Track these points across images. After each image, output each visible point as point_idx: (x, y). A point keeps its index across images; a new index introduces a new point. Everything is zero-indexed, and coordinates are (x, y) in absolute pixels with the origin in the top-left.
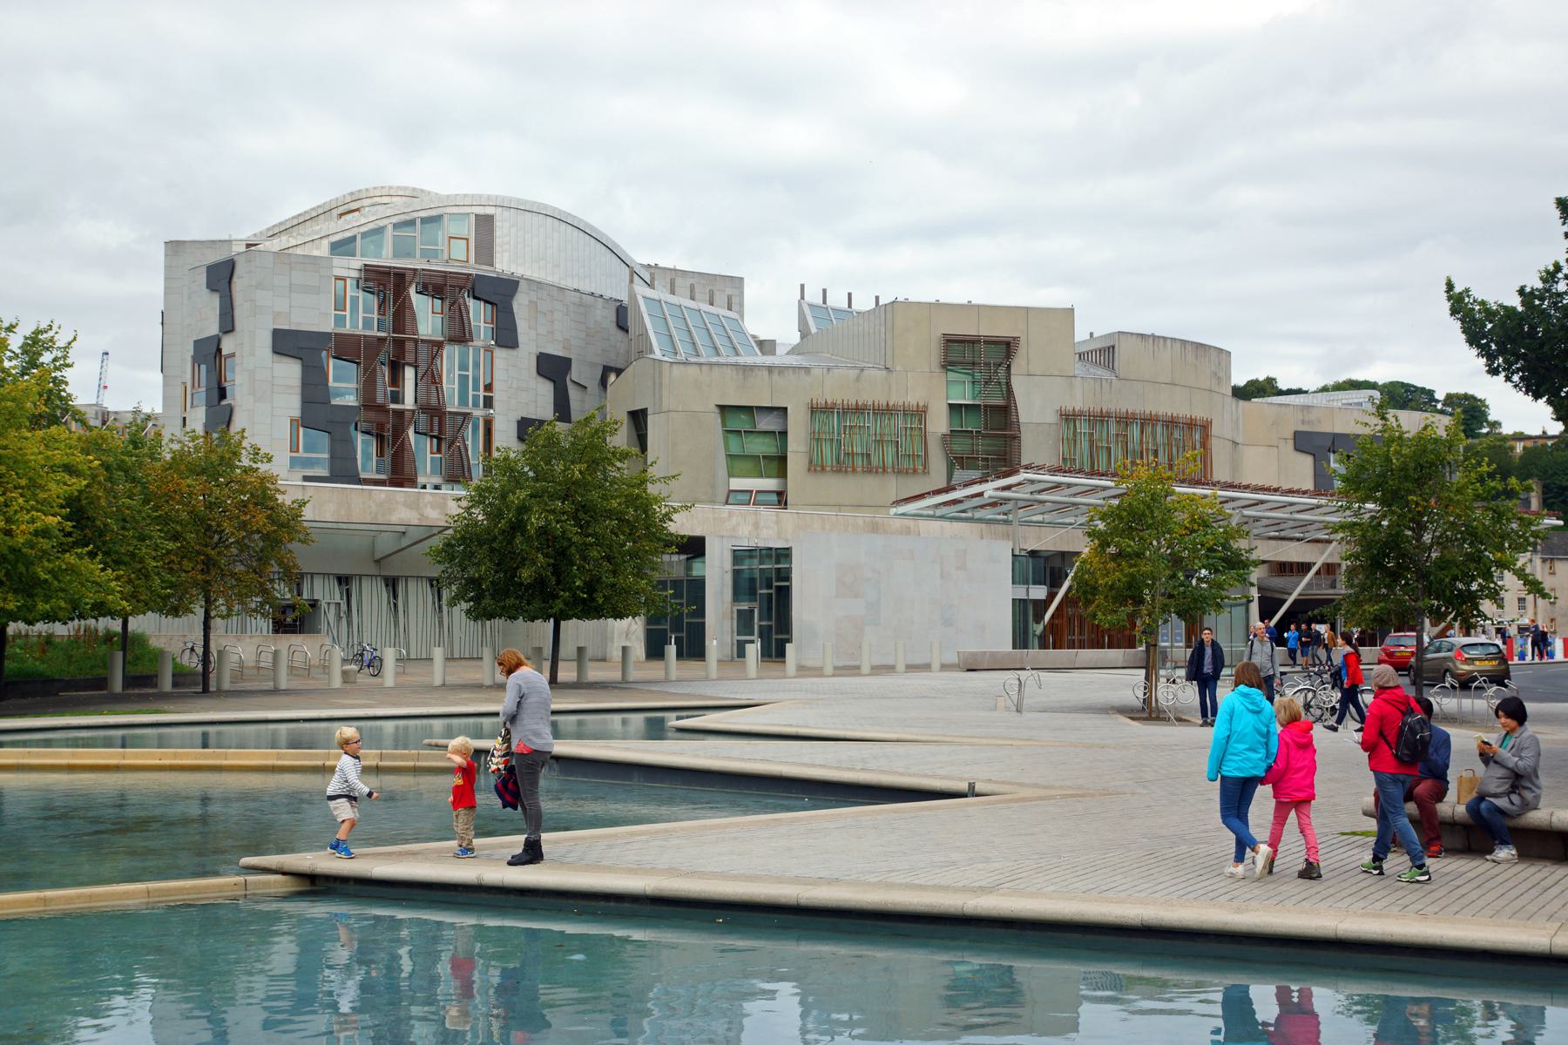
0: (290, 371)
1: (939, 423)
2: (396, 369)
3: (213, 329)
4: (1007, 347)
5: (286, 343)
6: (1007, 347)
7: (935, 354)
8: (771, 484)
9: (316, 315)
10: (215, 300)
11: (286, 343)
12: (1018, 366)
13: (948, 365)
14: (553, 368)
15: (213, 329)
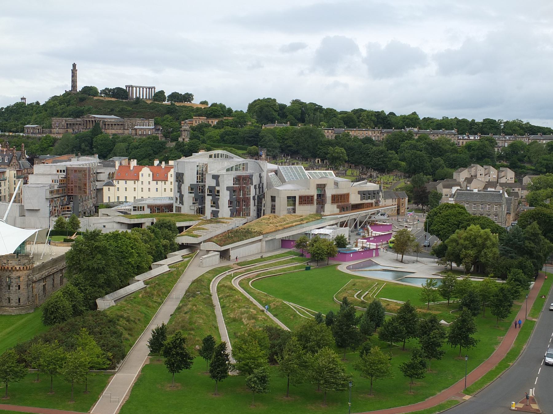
0: (229, 192)
1: (315, 197)
2: (240, 190)
3: (214, 185)
4: (324, 185)
5: (228, 188)
6: (324, 185)
7: (315, 187)
8: (291, 207)
9: (231, 184)
10: (215, 181)
11: (228, 188)
12: (326, 188)
13: (317, 188)
14: (255, 186)
15: (214, 185)
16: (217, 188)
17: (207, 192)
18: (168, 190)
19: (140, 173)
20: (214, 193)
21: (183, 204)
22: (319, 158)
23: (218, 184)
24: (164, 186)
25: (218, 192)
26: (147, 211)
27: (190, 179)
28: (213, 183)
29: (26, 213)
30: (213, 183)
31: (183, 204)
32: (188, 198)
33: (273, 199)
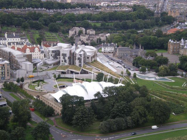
16: (81, 58)
17: (77, 59)
18: (35, 55)
19: (26, 50)
20: (79, 59)
21: (66, 62)
22: (14, 25)
23: (81, 57)
24: (34, 54)
25: (81, 59)
26: (52, 65)
27: (68, 55)
28: (80, 57)
29: (28, 72)
30: (80, 57)
31: (66, 62)
32: (68, 61)
33: (88, 58)
